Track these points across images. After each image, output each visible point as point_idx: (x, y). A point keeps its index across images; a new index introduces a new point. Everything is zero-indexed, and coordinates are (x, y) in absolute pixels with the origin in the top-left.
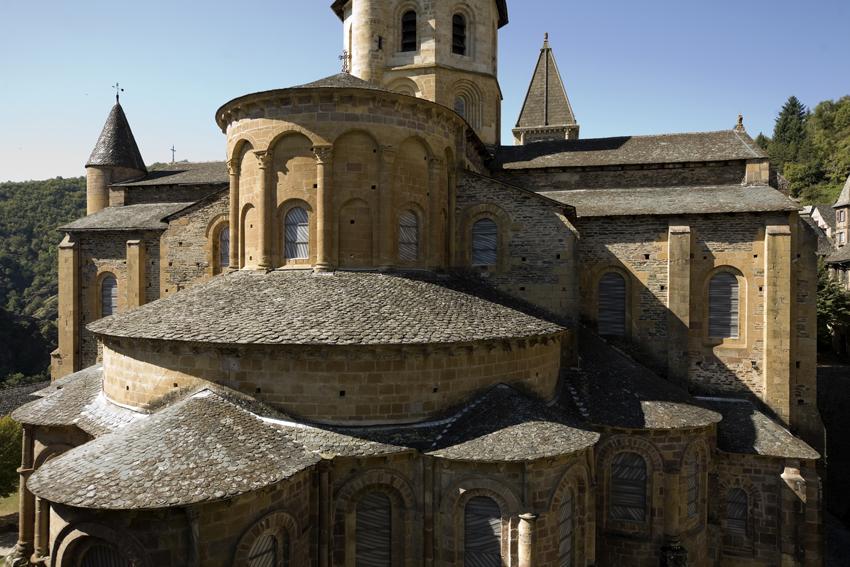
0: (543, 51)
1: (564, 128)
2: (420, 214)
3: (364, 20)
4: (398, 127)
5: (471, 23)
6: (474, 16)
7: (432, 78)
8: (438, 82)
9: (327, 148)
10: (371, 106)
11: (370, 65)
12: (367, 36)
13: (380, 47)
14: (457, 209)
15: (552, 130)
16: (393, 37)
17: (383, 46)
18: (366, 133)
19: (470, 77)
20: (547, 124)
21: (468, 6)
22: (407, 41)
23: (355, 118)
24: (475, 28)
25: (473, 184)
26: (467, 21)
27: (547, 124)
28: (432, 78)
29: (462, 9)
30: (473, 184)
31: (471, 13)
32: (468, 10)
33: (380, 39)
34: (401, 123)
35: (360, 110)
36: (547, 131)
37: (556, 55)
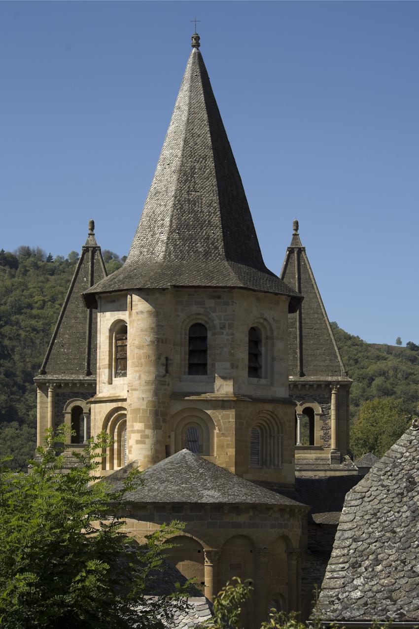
0: (291, 251)
1: (330, 383)
2: (281, 602)
3: (149, 339)
4: (270, 530)
5: (267, 338)
6: (271, 330)
7: (231, 414)
8: (238, 417)
9: (216, 553)
10: (251, 513)
11: (156, 393)
12: (153, 358)
13: (167, 371)
14: (302, 590)
15: (311, 386)
16: (180, 357)
17: (170, 369)
18: (247, 538)
19: (269, 407)
20: (302, 375)
21: (265, 319)
22: (196, 361)
23: (238, 525)
24: (273, 346)
25: (318, 567)
26: (263, 336)
27: (302, 375)
28: (231, 414)
29: (262, 324)
30: (318, 567)
31: (268, 327)
32: (265, 323)
33: (167, 359)
34: (273, 526)
35: (242, 519)
36: (304, 386)
37: (312, 257)
